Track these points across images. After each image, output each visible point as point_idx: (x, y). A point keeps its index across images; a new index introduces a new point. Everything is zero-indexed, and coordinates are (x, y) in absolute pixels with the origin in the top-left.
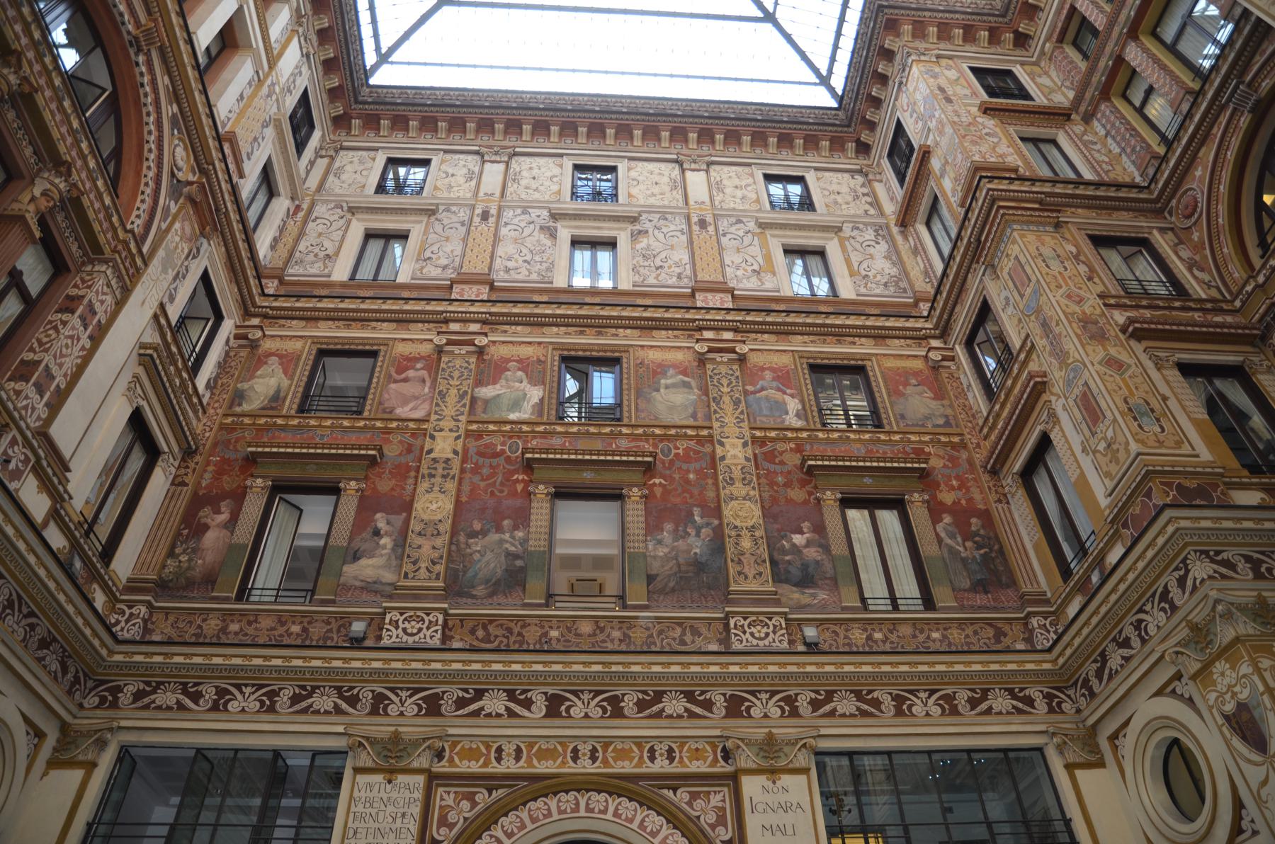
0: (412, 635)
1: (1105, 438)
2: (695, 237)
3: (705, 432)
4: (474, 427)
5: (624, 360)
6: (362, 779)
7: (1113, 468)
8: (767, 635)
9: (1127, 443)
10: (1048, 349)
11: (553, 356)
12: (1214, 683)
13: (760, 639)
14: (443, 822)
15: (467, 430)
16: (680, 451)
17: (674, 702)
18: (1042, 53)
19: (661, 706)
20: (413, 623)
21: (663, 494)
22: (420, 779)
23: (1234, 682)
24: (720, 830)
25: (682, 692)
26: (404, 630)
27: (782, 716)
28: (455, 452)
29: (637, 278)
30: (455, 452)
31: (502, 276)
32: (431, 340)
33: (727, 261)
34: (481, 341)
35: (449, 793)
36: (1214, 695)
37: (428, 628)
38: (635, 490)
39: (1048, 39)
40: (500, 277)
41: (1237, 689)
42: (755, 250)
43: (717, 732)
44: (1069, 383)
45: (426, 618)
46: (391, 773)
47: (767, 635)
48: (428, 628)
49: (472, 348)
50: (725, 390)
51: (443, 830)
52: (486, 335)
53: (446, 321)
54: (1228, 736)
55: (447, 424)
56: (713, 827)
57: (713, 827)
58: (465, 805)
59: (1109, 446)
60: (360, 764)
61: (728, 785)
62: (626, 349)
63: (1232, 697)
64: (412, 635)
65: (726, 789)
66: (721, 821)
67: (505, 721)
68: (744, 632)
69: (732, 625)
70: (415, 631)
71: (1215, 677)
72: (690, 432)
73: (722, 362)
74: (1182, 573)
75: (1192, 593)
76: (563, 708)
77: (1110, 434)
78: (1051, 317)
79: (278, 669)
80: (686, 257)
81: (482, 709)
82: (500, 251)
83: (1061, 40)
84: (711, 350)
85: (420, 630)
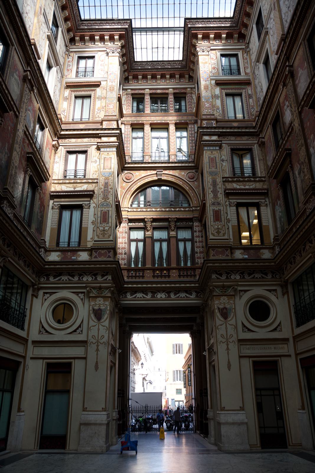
1: (104, 228)
7: (101, 236)
9: (111, 235)
10: (102, 190)
12: (96, 301)
18: (126, 89)
23: (102, 304)
36: (94, 303)
39: (132, 89)
41: (102, 306)
44: (103, 205)
54: (91, 313)
59: (104, 230)
63: (99, 306)
71: (97, 300)
74: (105, 274)
75: (104, 280)
77: (107, 228)
78: (110, 185)
83: (132, 94)
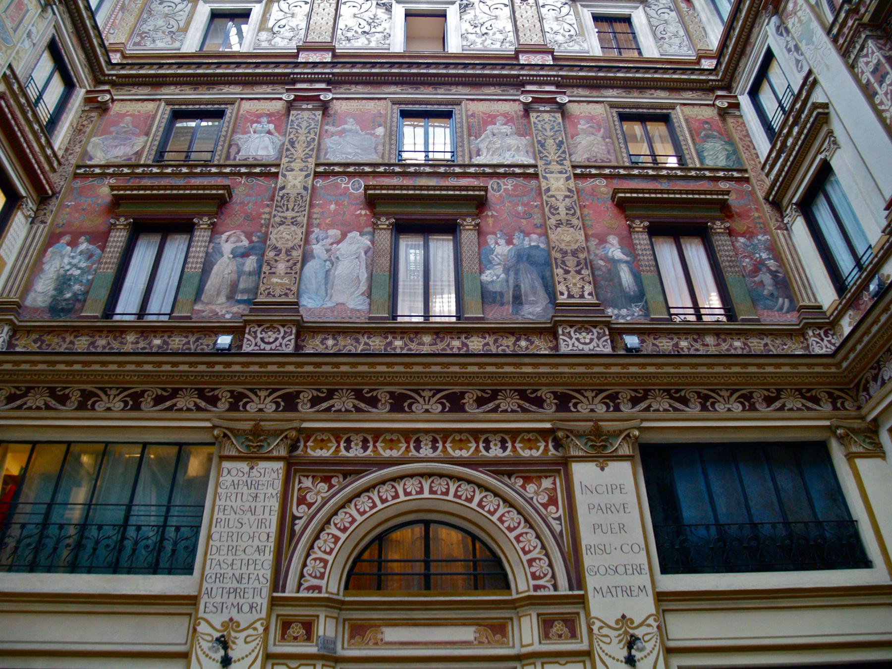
0: (269, 343)
2: (516, 8)
3: (531, 171)
4: (321, 169)
5: (457, 112)
6: (226, 465)
8: (592, 340)
11: (392, 110)
13: (585, 344)
14: (302, 501)
15: (315, 172)
16: (510, 187)
17: (508, 400)
19: (497, 402)
20: (270, 333)
21: (494, 222)
22: (280, 465)
24: (552, 508)
25: (516, 391)
26: (262, 339)
27: (607, 411)
28: (305, 188)
29: (465, 43)
30: (305, 188)
31: (345, 44)
32: (281, 99)
33: (547, 29)
34: (326, 96)
35: (308, 477)
37: (283, 338)
38: (469, 220)
40: (342, 47)
42: (571, 19)
43: (548, 425)
45: (282, 330)
46: (252, 458)
47: (592, 340)
48: (283, 338)
49: (317, 104)
50: (549, 133)
51: (303, 508)
52: (329, 90)
53: (294, 82)
55: (296, 165)
56: (545, 506)
57: (545, 506)
58: (323, 486)
60: (226, 453)
61: (558, 471)
62: (458, 103)
64: (269, 343)
65: (556, 475)
66: (553, 501)
67: (354, 416)
68: (571, 338)
69: (560, 332)
70: (271, 340)
72: (517, 170)
73: (545, 111)
76: (406, 404)
79: (147, 374)
80: (509, 27)
81: (333, 406)
82: (341, 24)
84: (536, 101)
85: (276, 339)
